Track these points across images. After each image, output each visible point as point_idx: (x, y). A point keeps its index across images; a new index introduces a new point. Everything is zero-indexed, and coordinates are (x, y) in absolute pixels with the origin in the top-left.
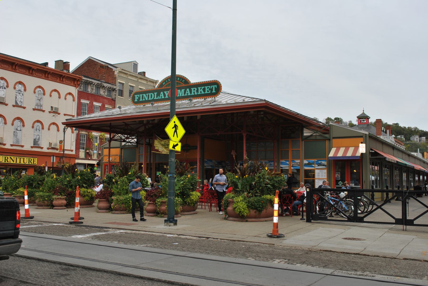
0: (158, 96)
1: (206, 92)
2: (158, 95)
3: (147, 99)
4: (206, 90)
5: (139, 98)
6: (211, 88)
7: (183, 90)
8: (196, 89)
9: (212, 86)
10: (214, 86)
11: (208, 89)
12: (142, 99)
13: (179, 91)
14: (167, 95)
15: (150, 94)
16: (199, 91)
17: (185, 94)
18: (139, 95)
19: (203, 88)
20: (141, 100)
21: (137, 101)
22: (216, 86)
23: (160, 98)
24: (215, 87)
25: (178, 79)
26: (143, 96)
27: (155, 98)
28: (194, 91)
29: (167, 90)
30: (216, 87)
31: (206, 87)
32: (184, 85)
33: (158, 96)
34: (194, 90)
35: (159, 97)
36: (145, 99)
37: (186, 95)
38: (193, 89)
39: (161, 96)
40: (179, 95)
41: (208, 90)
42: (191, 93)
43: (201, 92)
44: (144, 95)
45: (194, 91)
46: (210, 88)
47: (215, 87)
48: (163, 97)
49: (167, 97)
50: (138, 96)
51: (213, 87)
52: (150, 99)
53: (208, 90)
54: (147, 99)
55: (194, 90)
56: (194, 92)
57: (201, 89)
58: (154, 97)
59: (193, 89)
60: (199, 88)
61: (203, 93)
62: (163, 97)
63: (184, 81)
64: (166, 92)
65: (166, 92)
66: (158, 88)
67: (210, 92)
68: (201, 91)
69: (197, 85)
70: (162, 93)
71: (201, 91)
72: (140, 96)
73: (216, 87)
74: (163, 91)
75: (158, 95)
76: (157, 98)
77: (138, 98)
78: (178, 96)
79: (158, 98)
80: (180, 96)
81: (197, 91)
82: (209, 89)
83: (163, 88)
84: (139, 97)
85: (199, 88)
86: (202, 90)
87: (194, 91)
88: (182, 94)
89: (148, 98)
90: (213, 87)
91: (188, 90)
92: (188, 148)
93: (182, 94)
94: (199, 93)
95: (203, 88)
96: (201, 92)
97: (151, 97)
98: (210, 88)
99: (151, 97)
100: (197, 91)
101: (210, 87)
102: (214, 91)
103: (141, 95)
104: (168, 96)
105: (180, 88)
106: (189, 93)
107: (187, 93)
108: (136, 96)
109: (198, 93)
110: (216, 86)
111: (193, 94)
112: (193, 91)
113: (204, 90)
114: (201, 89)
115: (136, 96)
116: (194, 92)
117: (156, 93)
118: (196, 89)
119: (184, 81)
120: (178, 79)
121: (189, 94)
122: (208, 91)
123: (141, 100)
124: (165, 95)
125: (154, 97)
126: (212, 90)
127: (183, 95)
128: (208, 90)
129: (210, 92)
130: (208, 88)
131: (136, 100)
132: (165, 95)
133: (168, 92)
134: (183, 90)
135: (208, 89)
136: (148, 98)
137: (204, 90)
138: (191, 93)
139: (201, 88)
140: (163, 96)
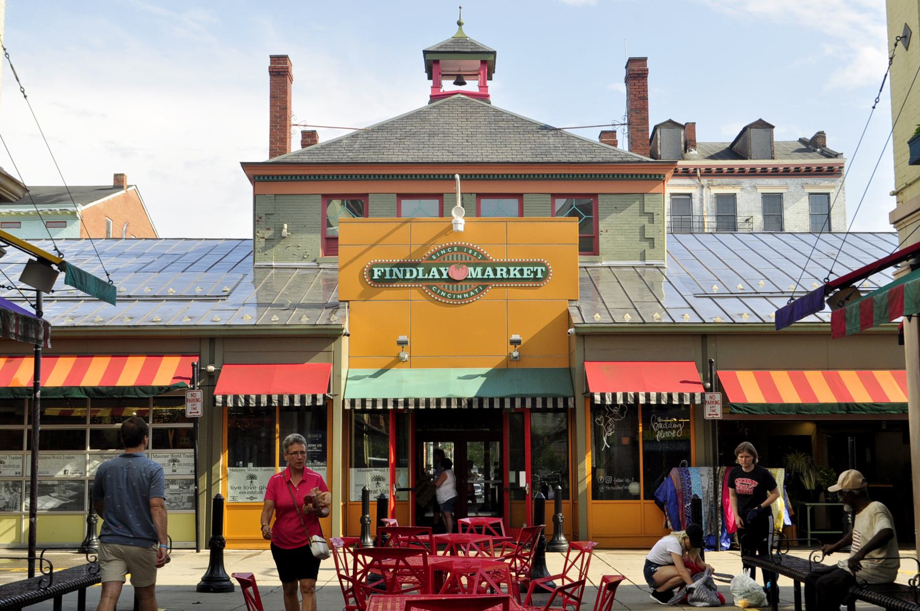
1: (525, 276)
3: (401, 276)
4: (526, 272)
5: (384, 274)
7: (479, 269)
9: (535, 268)
10: (539, 269)
12: (391, 274)
13: (471, 269)
14: (445, 273)
15: (408, 269)
16: (512, 273)
17: (483, 274)
19: (518, 268)
20: (388, 277)
21: (378, 278)
22: (544, 269)
23: (431, 277)
24: (542, 270)
27: (420, 276)
30: (544, 270)
34: (502, 270)
35: (429, 276)
36: (396, 275)
37: (485, 277)
39: (431, 274)
40: (471, 275)
41: (529, 272)
43: (515, 275)
47: (542, 270)
48: (437, 276)
49: (445, 276)
51: (537, 270)
52: (408, 276)
55: (502, 270)
56: (502, 274)
57: (515, 270)
59: (498, 269)
60: (512, 269)
61: (518, 276)
62: (437, 276)
64: (442, 269)
67: (532, 276)
70: (434, 269)
72: (385, 271)
74: (437, 266)
78: (470, 277)
79: (426, 277)
80: (474, 276)
81: (508, 272)
82: (531, 272)
84: (383, 271)
86: (516, 272)
87: (501, 272)
88: (477, 275)
90: (537, 270)
91: (489, 269)
93: (477, 275)
94: (512, 276)
95: (518, 268)
97: (411, 274)
99: (411, 274)
100: (508, 272)
101: (532, 268)
104: (448, 274)
105: (475, 265)
107: (486, 273)
109: (509, 275)
110: (544, 269)
111: (499, 276)
112: (499, 272)
113: (521, 272)
114: (515, 270)
115: (376, 270)
116: (502, 274)
117: (421, 269)
118: (505, 269)
121: (492, 276)
122: (528, 275)
123: (388, 277)
124: (440, 273)
125: (418, 275)
126: (536, 273)
127: (480, 276)
129: (532, 276)
130: (528, 270)
131: (376, 277)
132: (440, 273)
134: (479, 269)
136: (405, 274)
137: (521, 272)
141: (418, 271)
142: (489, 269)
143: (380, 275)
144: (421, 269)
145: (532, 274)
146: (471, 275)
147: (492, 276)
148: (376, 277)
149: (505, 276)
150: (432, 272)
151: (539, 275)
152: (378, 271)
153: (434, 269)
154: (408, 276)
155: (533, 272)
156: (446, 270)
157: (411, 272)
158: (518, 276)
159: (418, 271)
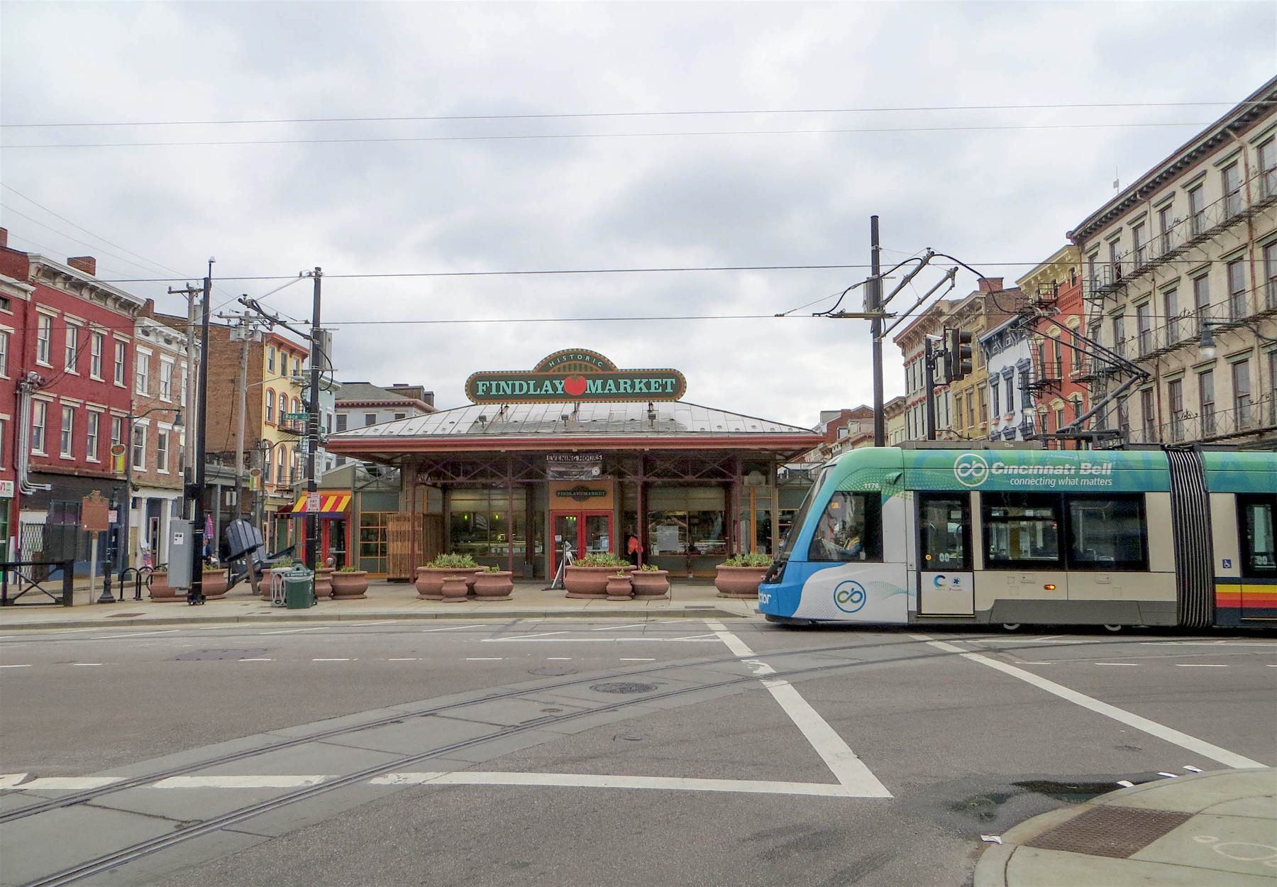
1: (653, 390)
3: (509, 392)
4: (653, 385)
5: (490, 389)
6: (664, 383)
7: (599, 382)
9: (664, 380)
10: (669, 381)
12: (498, 390)
13: (590, 382)
14: (560, 388)
15: (517, 383)
16: (637, 386)
17: (603, 389)
18: (488, 383)
19: (644, 381)
22: (674, 380)
23: (543, 392)
24: (672, 382)
25: (588, 358)
27: (532, 392)
29: (560, 378)
30: (674, 383)
31: (653, 381)
32: (600, 372)
34: (625, 383)
36: (504, 390)
37: (606, 391)
38: (622, 381)
39: (544, 388)
40: (590, 390)
41: (657, 385)
42: (618, 387)
43: (641, 389)
46: (661, 383)
47: (672, 382)
49: (560, 391)
51: (666, 382)
52: (517, 392)
54: (509, 392)
56: (625, 389)
57: (640, 383)
58: (528, 390)
59: (622, 381)
60: (637, 381)
61: (645, 390)
62: (551, 392)
64: (557, 382)
65: (557, 382)
66: (538, 371)
67: (660, 390)
68: (640, 386)
69: (632, 375)
70: (547, 383)
72: (491, 385)
73: (674, 383)
74: (551, 378)
78: (588, 392)
79: (538, 392)
83: (551, 372)
85: (637, 381)
86: (642, 385)
87: (625, 385)
88: (597, 390)
89: (513, 390)
90: (666, 382)
91: (611, 382)
92: (586, 494)
93: (597, 390)
94: (637, 390)
95: (644, 381)
96: (641, 389)
97: (521, 389)
98: (661, 383)
99: (521, 389)
100: (633, 386)
101: (660, 380)
102: (669, 390)
103: (494, 383)
106: (613, 387)
107: (608, 387)
108: (480, 384)
110: (674, 380)
113: (648, 385)
114: (640, 383)
115: (480, 384)
116: (625, 389)
117: (532, 383)
118: (629, 382)
120: (588, 358)
121: (614, 391)
123: (494, 392)
124: (555, 388)
125: (528, 390)
126: (665, 387)
127: (600, 391)
129: (660, 390)
131: (480, 393)
132: (555, 388)
133: (563, 381)
134: (599, 382)
136: (513, 390)
140: (549, 388)
142: (611, 382)
147: (614, 391)
148: (480, 393)
153: (547, 383)
154: (517, 392)
157: (521, 386)
158: (645, 390)
159: (528, 384)
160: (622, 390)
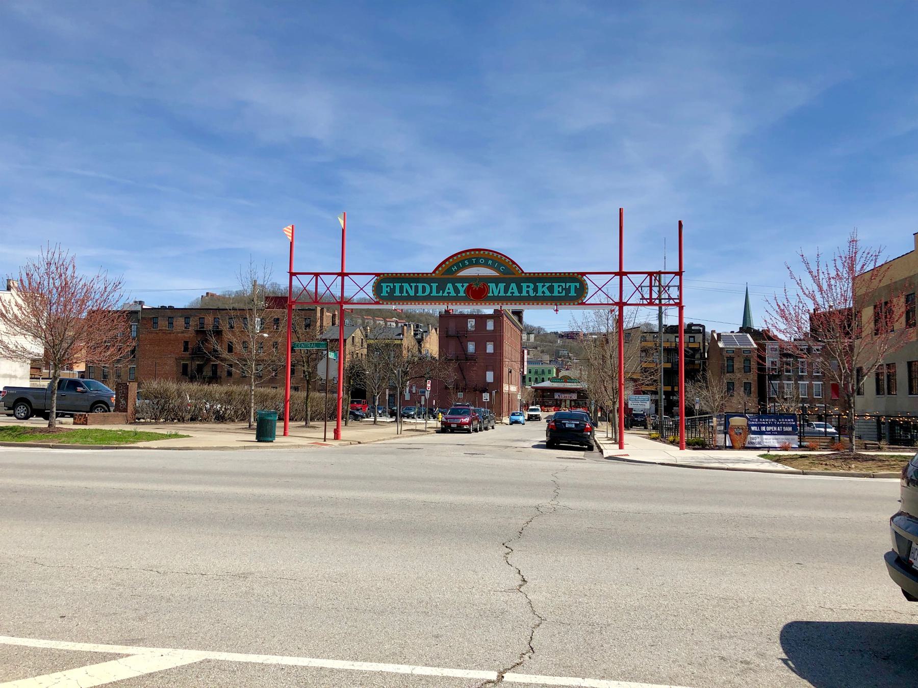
0: (441, 291)
1: (556, 294)
2: (441, 288)
3: (412, 293)
4: (556, 289)
5: (393, 290)
6: (567, 287)
7: (502, 286)
8: (532, 286)
9: (568, 285)
10: (573, 285)
11: (559, 287)
12: (401, 291)
15: (420, 285)
16: (540, 290)
17: (506, 292)
18: (391, 285)
22: (578, 285)
23: (445, 294)
24: (576, 286)
25: (490, 262)
26: (401, 288)
27: (434, 294)
28: (528, 289)
30: (578, 287)
31: (556, 285)
33: (441, 291)
34: (528, 287)
35: (443, 293)
36: (407, 292)
37: (509, 294)
38: (524, 285)
39: (447, 290)
40: (493, 293)
41: (560, 289)
42: (520, 291)
43: (543, 292)
44: (406, 286)
45: (528, 289)
46: (564, 287)
47: (576, 286)
49: (462, 294)
50: (390, 286)
51: (570, 286)
52: (420, 294)
53: (559, 291)
54: (412, 293)
55: (528, 287)
56: (528, 292)
57: (543, 286)
58: (431, 292)
59: (524, 285)
61: (548, 294)
62: (453, 294)
63: (502, 269)
64: (459, 285)
65: (459, 285)
67: (563, 294)
70: (450, 285)
71: (542, 289)
72: (394, 287)
73: (578, 287)
75: (441, 288)
76: (437, 295)
77: (388, 289)
78: (490, 294)
79: (440, 294)
80: (496, 294)
81: (535, 289)
84: (392, 287)
85: (540, 285)
88: (499, 293)
89: (416, 291)
90: (570, 286)
91: (513, 285)
93: (499, 293)
94: (540, 294)
95: (547, 285)
96: (543, 292)
98: (564, 287)
100: (535, 289)
101: (563, 285)
102: (573, 294)
103: (398, 285)
106: (516, 290)
107: (510, 290)
108: (384, 285)
109: (537, 293)
110: (578, 285)
111: (524, 294)
112: (525, 290)
113: (551, 289)
114: (543, 286)
115: (384, 285)
116: (528, 292)
117: (434, 285)
118: (532, 286)
119: (502, 269)
121: (517, 294)
122: (559, 293)
123: (397, 294)
124: (457, 290)
125: (431, 292)
126: (568, 290)
127: (502, 294)
128: (559, 291)
129: (563, 294)
131: (384, 294)
132: (457, 290)
134: (502, 286)
135: (559, 287)
136: (416, 291)
137: (551, 289)
138: (520, 291)
139: (543, 284)
140: (452, 290)
141: (431, 287)
143: (389, 291)
144: (434, 285)
145: (564, 291)
146: (493, 293)
147: (517, 294)
149: (532, 294)
150: (447, 288)
151: (573, 294)
152: (387, 286)
153: (450, 285)
154: (420, 294)
155: (565, 289)
156: (463, 286)
158: (548, 294)
159: (431, 287)
160: (524, 294)
